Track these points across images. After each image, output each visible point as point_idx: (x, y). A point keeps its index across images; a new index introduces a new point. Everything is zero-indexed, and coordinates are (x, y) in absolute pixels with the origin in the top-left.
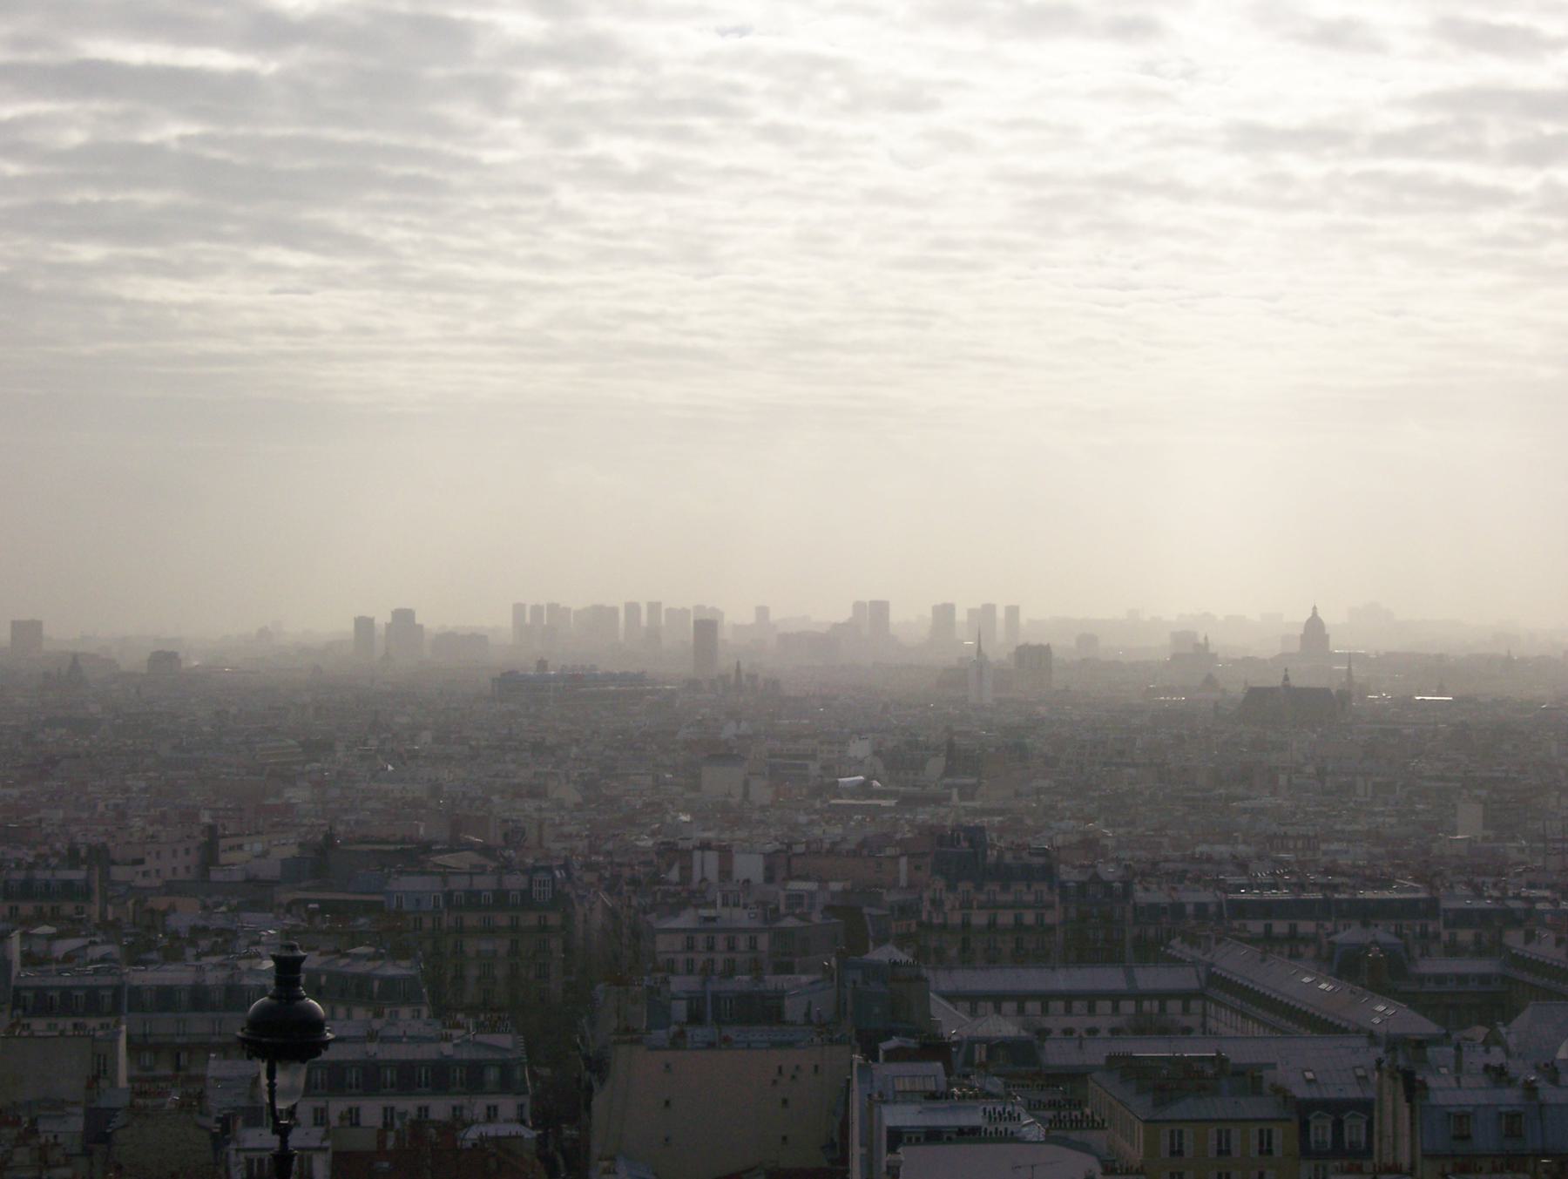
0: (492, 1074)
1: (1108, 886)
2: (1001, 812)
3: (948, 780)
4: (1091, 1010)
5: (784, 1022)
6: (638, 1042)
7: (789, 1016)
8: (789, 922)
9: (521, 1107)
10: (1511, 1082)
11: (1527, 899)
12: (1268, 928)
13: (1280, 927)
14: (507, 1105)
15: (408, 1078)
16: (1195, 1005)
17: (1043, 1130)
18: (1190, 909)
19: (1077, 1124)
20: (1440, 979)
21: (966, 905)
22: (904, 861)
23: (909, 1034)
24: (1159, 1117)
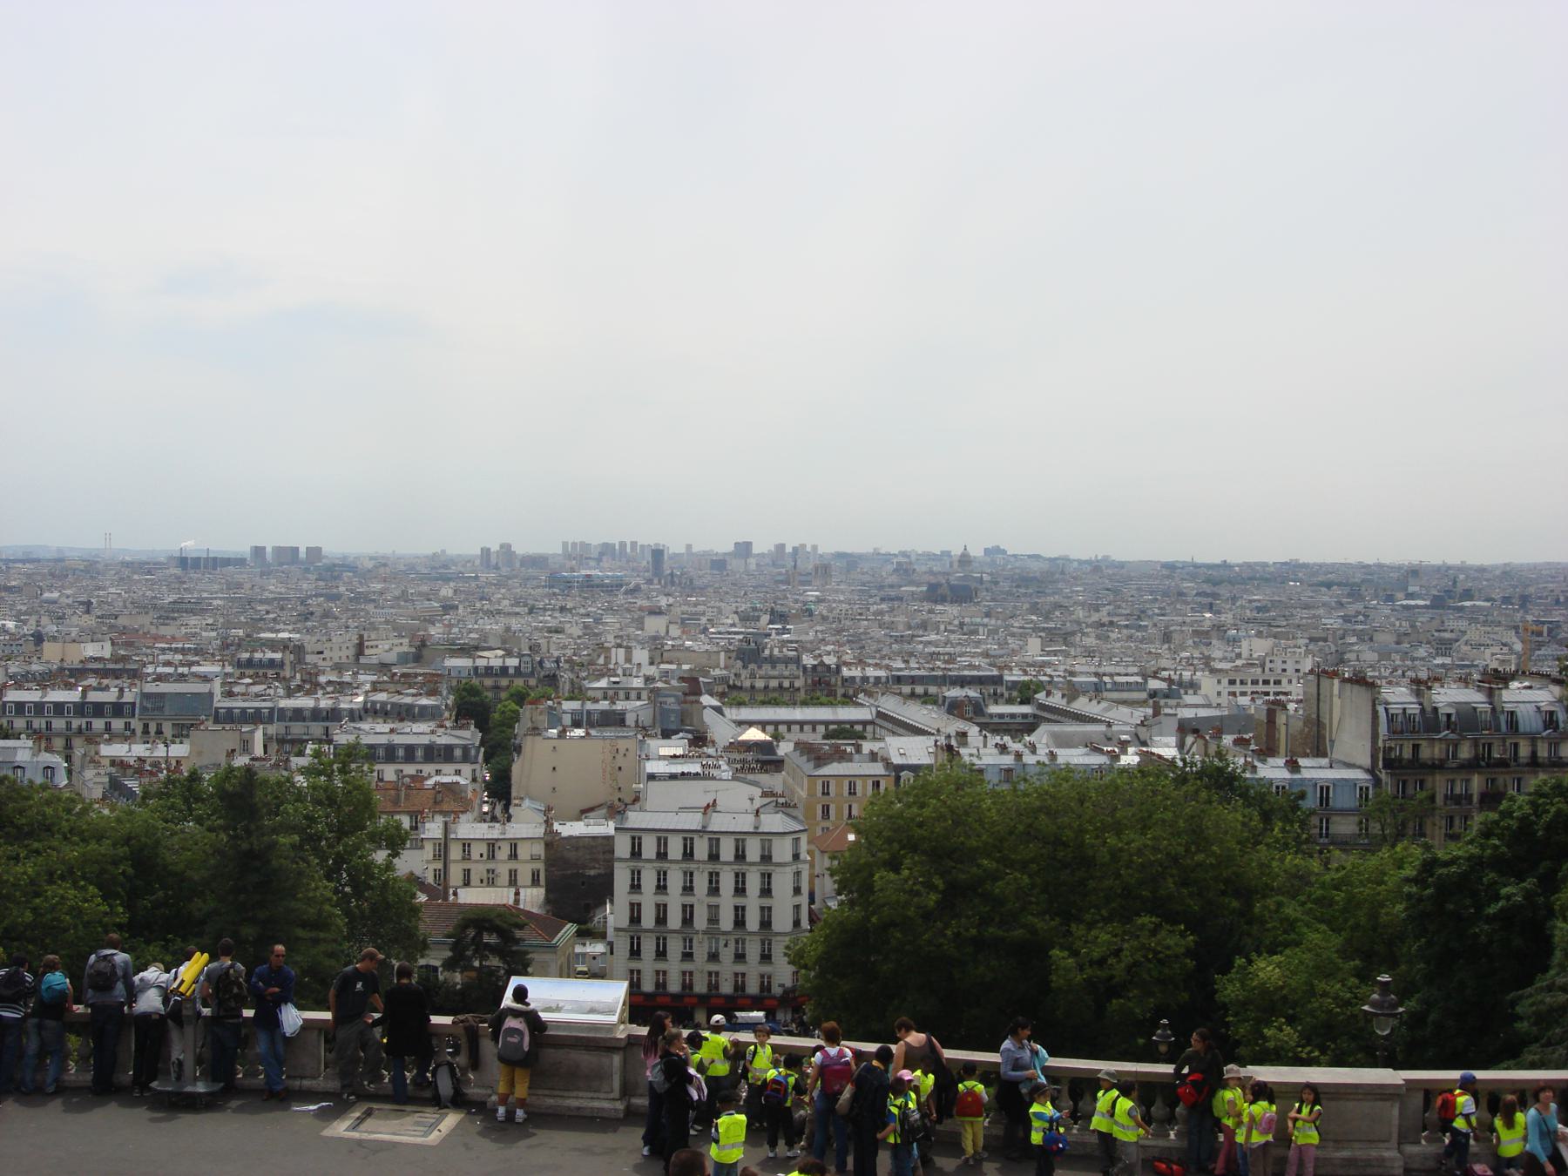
0: (458, 753)
1: (828, 667)
2: (797, 642)
3: (771, 626)
4: (814, 730)
5: (625, 726)
6: (540, 734)
7: (628, 723)
8: (659, 685)
9: (474, 771)
10: (1008, 753)
11: (1050, 676)
12: (913, 689)
13: (919, 690)
14: (467, 769)
15: (410, 753)
16: (870, 728)
17: (731, 774)
18: (872, 680)
19: (752, 770)
20: (1001, 716)
21: (753, 676)
22: (723, 653)
23: (687, 731)
24: (816, 774)
